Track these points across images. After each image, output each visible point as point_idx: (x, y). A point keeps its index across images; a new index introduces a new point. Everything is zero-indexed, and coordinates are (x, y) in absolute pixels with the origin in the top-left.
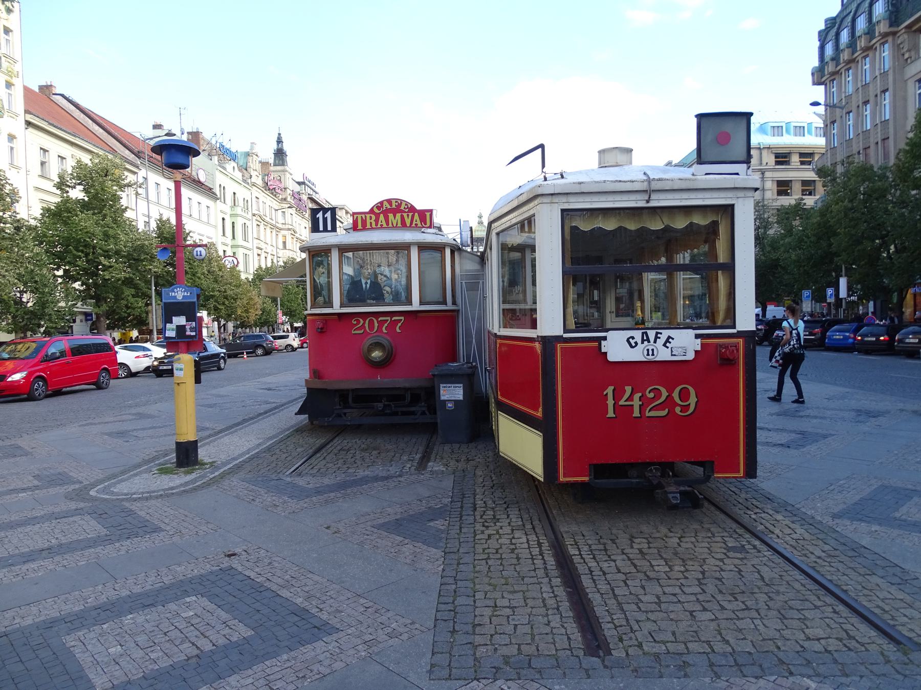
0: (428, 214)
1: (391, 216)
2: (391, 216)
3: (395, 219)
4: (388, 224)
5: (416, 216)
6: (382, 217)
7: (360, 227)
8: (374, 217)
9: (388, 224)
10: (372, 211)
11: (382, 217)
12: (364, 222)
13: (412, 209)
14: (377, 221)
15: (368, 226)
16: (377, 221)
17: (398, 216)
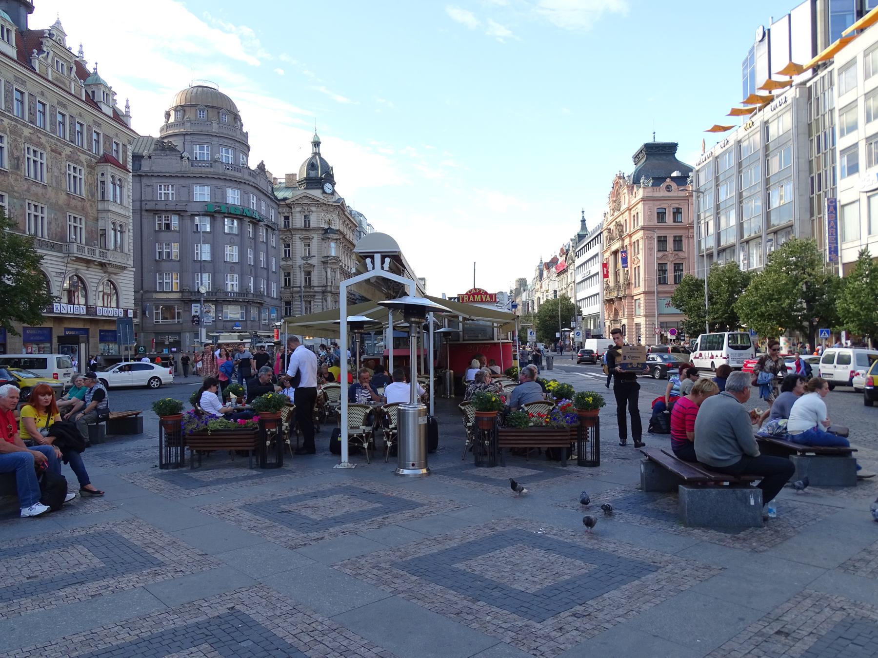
0: (494, 296)
1: (476, 296)
2: (476, 296)
3: (478, 298)
4: (474, 300)
5: (488, 296)
6: (471, 297)
7: (461, 301)
8: (467, 297)
9: (474, 300)
10: (467, 294)
11: (471, 297)
12: (463, 299)
13: (486, 293)
14: (469, 298)
15: (465, 301)
16: (469, 298)
17: (479, 296)
